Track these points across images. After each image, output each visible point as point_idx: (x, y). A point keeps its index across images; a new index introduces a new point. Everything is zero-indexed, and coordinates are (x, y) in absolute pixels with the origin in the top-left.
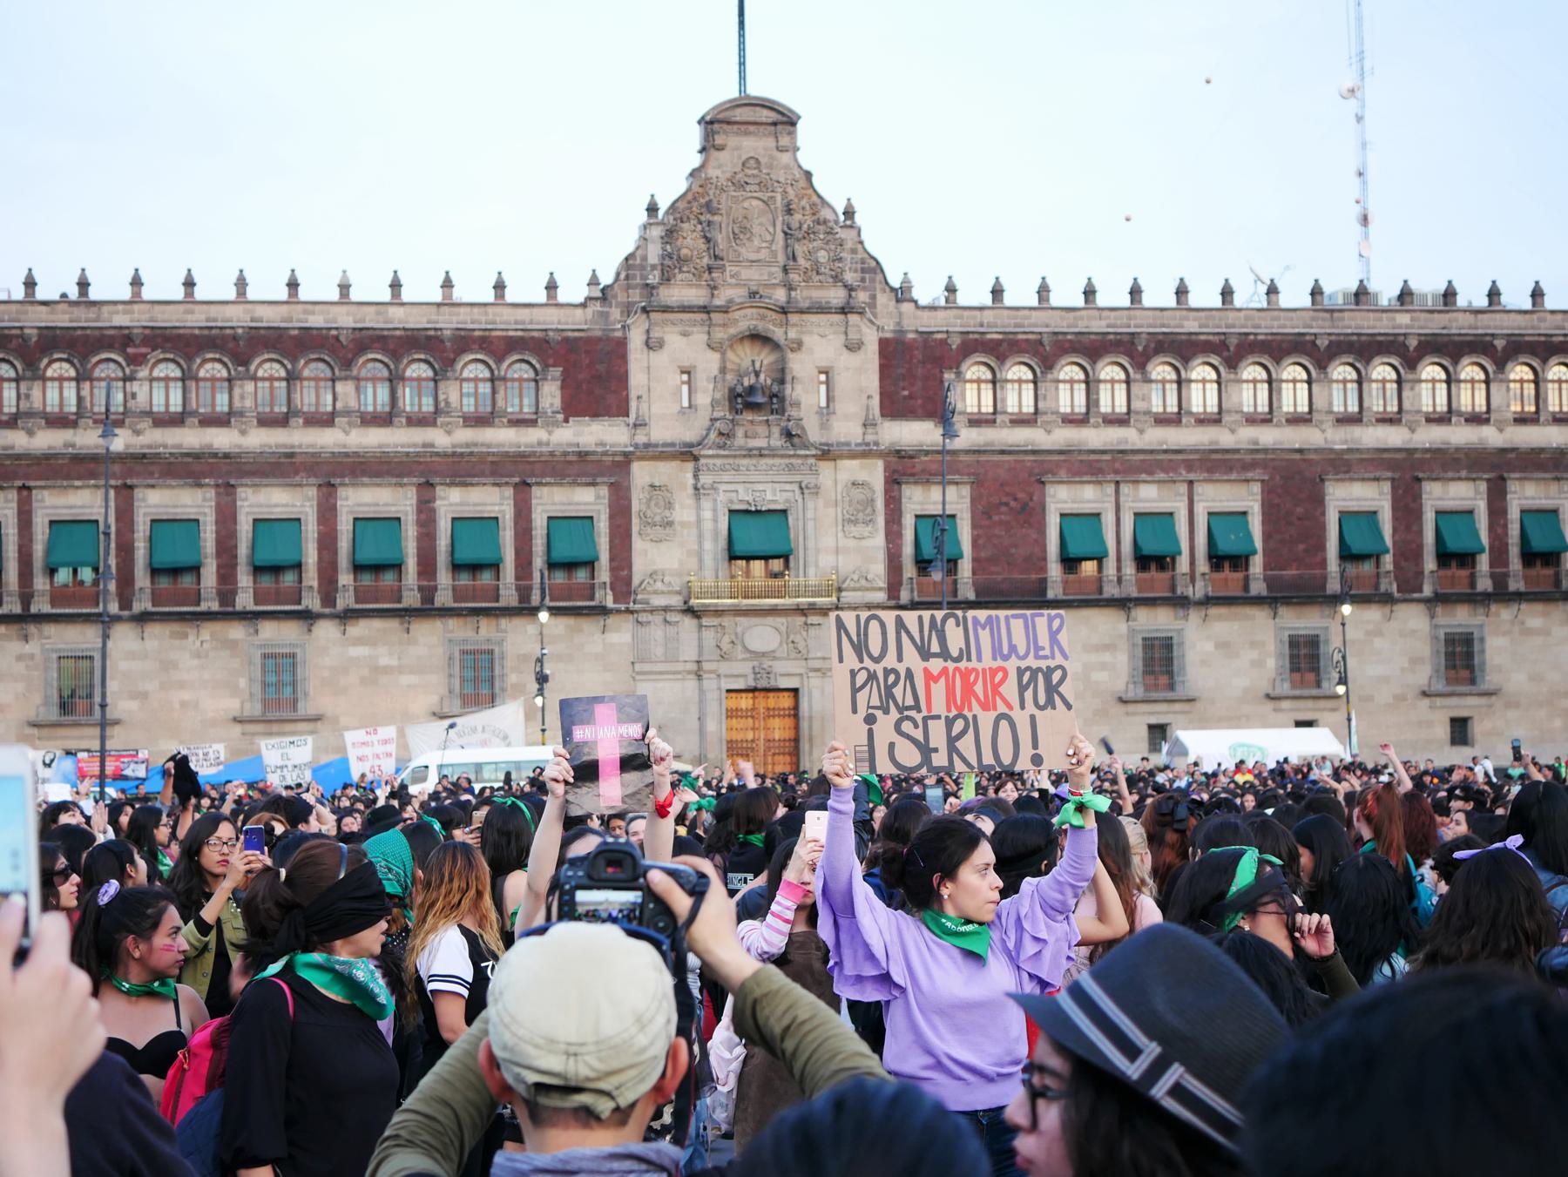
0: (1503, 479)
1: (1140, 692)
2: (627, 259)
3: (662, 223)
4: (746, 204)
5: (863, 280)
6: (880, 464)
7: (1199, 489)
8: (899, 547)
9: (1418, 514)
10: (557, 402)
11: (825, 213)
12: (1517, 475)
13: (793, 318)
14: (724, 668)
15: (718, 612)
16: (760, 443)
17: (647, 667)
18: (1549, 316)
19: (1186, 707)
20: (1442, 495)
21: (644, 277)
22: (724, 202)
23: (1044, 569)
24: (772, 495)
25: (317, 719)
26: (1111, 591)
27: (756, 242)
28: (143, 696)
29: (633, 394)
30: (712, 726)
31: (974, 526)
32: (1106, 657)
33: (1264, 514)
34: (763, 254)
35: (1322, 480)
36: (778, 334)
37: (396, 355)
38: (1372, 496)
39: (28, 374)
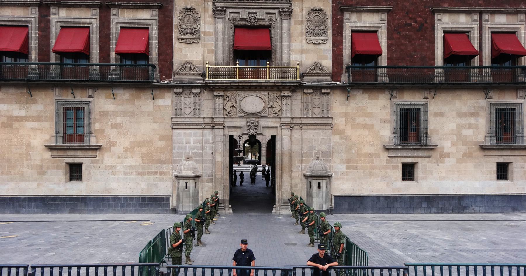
1: (494, 143)
8: (341, 51)
14: (228, 123)
15: (226, 88)
17: (180, 121)
26: (475, 79)
30: (219, 158)
31: (389, 38)
32: (472, 120)
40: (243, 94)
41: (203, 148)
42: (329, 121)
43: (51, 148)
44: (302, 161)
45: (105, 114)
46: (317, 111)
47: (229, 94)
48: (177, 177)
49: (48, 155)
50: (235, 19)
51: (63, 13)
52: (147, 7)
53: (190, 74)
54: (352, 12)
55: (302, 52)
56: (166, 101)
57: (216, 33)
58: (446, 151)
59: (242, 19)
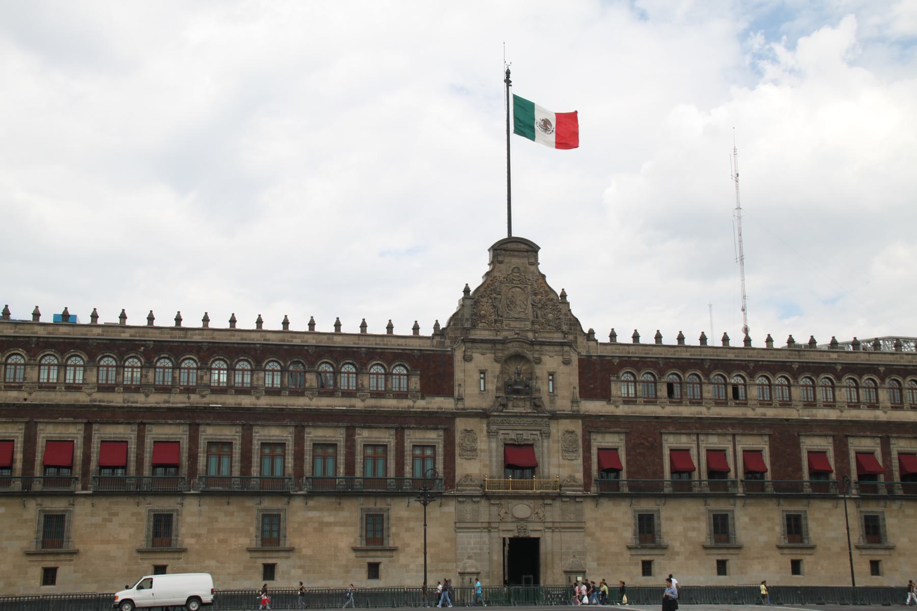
0: (889, 437)
2: (454, 315)
3: (471, 298)
4: (513, 290)
5: (570, 329)
6: (580, 422)
7: (738, 438)
8: (590, 465)
9: (847, 454)
10: (418, 387)
11: (552, 296)
12: (895, 435)
13: (537, 348)
14: (503, 527)
15: (500, 497)
16: (522, 410)
17: (462, 525)
18: (905, 356)
19: (736, 551)
20: (857, 444)
21: (462, 325)
22: (504, 289)
23: (662, 477)
24: (527, 436)
25: (291, 550)
26: (696, 490)
27: (519, 309)
28: (198, 536)
29: (456, 384)
32: (695, 524)
33: (770, 452)
34: (522, 315)
35: (799, 435)
36: (529, 355)
37: (337, 361)
38: (824, 444)
39: (147, 365)
40: (514, 502)
41: (481, 549)
42: (583, 525)
43: (355, 550)
44: (561, 559)
45: (400, 519)
46: (572, 516)
47: (503, 502)
48: (461, 574)
49: (352, 555)
50: (505, 439)
51: (366, 433)
52: (436, 429)
53: (471, 486)
54: (598, 432)
55: (559, 466)
56: (450, 508)
57: (490, 451)
58: (676, 550)
59: (511, 439)
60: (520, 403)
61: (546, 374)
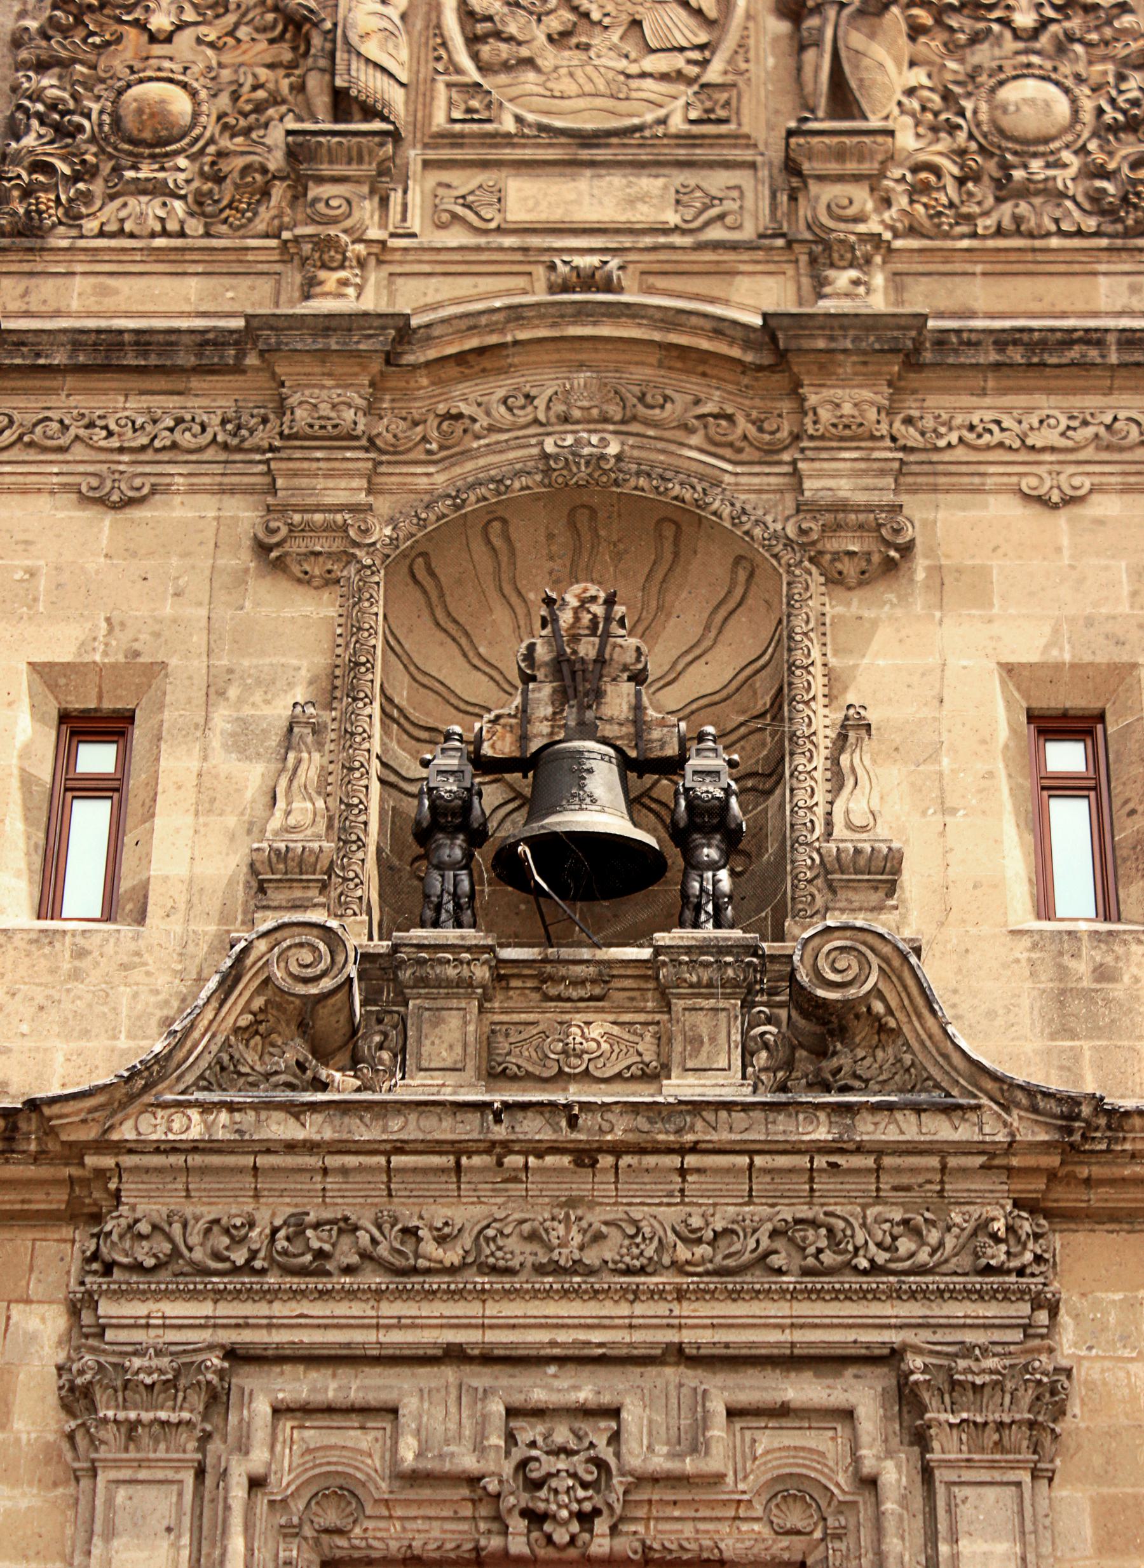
36: (749, 492)
60: (594, 1031)
61: (1000, 719)
